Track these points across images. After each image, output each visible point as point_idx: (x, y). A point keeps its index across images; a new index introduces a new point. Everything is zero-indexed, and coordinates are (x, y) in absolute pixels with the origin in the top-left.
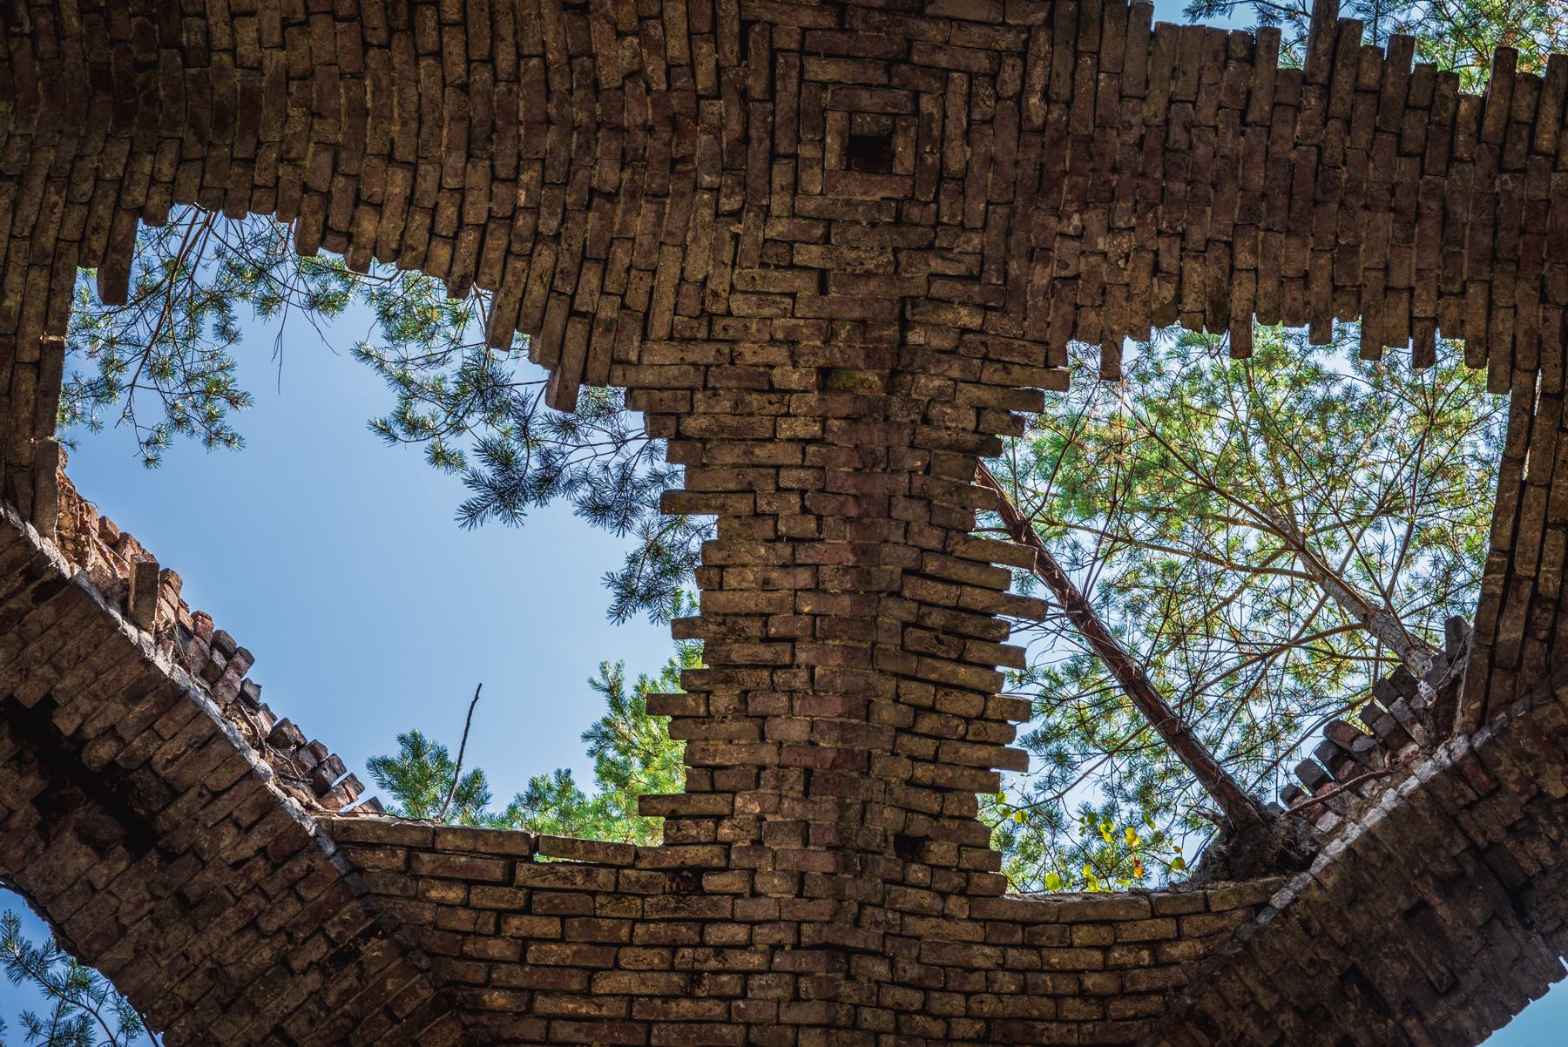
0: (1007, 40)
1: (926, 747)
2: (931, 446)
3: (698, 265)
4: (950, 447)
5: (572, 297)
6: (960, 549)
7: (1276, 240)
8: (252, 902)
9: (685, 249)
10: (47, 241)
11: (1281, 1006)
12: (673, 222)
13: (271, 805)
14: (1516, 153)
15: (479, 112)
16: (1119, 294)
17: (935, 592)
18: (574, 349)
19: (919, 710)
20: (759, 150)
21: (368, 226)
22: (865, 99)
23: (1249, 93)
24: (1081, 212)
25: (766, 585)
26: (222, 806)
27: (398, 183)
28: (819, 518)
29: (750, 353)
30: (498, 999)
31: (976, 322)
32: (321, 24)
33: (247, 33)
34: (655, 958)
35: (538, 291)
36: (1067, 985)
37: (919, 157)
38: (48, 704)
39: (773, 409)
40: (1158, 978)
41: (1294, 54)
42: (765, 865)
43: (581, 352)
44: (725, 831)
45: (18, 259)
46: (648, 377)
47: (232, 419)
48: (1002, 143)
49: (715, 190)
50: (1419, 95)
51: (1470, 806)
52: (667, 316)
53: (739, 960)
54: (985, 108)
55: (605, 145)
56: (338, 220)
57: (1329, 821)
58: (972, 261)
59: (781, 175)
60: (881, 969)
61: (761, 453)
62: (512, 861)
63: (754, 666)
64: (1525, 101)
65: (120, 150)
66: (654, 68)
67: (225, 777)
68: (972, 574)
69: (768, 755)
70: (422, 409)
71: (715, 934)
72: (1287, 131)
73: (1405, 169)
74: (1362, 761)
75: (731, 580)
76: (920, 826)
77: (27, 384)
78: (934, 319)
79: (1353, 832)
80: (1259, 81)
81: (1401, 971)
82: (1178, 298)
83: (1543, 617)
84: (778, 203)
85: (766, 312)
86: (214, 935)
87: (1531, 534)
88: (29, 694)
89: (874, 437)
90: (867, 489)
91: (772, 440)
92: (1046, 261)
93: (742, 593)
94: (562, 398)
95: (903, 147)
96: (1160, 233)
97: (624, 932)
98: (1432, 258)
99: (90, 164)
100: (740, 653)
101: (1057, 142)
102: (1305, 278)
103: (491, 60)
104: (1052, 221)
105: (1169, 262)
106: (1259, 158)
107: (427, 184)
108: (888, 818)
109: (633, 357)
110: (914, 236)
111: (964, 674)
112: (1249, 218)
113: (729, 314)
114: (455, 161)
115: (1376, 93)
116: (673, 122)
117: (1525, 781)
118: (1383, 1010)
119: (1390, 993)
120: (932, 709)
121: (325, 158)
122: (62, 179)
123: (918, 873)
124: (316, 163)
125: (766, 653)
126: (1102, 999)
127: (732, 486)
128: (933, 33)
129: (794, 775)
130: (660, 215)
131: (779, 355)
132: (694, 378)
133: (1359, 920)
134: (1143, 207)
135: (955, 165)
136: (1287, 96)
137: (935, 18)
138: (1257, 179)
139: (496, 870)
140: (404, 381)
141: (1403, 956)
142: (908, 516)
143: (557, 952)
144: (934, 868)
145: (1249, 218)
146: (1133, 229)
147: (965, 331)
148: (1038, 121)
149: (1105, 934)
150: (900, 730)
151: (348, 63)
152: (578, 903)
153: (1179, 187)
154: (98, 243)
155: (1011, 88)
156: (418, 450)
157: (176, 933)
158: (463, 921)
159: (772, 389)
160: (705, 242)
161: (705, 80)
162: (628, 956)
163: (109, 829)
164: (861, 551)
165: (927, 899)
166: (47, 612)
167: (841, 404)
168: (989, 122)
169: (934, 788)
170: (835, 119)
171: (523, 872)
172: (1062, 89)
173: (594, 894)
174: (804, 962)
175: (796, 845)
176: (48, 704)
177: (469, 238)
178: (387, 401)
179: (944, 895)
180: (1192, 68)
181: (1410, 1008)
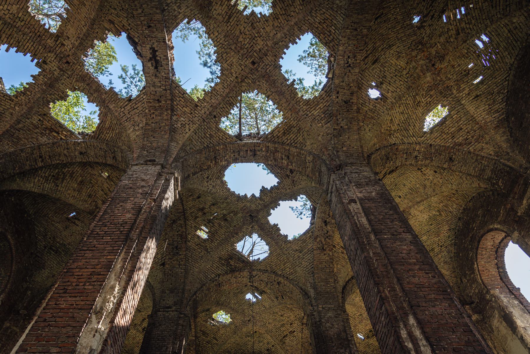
0: (270, 64)
1: (222, 111)
3: (234, 61)
7: (276, 95)
8: (161, 80)
10: (186, 14)
12: (235, 56)
13: (168, 74)
14: (298, 103)
15: (227, 34)
17: (232, 100)
19: (224, 107)
20: (246, 56)
21: (212, 35)
22: (256, 59)
26: (165, 71)
27: (217, 34)
29: (232, 71)
30: (175, 103)
32: (221, 16)
33: (215, 12)
34: (190, 109)
35: (221, 52)
36: (218, 136)
38: (157, 51)
40: (225, 141)
41: (289, 83)
42: (203, 109)
44: (202, 104)
45: (183, 13)
46: (223, 66)
47: (186, 40)
48: (263, 71)
50: (295, 93)
53: (196, 115)
54: (264, 67)
55: (235, 45)
56: (210, 33)
57: (246, 139)
59: (246, 59)
60: (206, 124)
61: (227, 79)
62: (184, 93)
65: (198, 12)
66: (243, 43)
67: (167, 69)
68: (235, 101)
69: (210, 101)
70: (201, 53)
71: (195, 111)
73: (290, 98)
74: (251, 137)
75: (217, 86)
76: (217, 116)
77: (175, 24)
79: (247, 141)
80: (285, 83)
81: (243, 154)
84: (244, 61)
86: (156, 80)
88: (156, 49)
89: (237, 85)
93: (217, 88)
94: (216, 61)
95: (256, 65)
98: (286, 106)
99: (195, 11)
100: (214, 92)
102: (276, 100)
103: (231, 31)
105: (268, 90)
107: (219, 36)
108: (215, 113)
111: (229, 107)
114: (223, 36)
116: (241, 48)
118: (239, 155)
119: (240, 155)
121: (213, 27)
122: (191, 10)
123: (214, 119)
124: (212, 27)
125: (216, 94)
128: (265, 58)
131: (235, 73)
132: (227, 69)
134: (269, 84)
135: (259, 70)
139: (182, 93)
140: (202, 49)
143: (182, 103)
151: (221, 21)
152: (187, 101)
153: (273, 85)
154: (190, 18)
155: (267, 67)
156: (198, 56)
157: (153, 77)
158: (177, 95)
161: (246, 47)
162: (187, 108)
163: (154, 65)
164: (229, 92)
165: (213, 122)
166: (163, 43)
167: (236, 80)
170: (253, 58)
171: (184, 95)
172: (271, 71)
174: (201, 119)
176: (157, 51)
177: (219, 43)
178: (199, 50)
181: (241, 157)
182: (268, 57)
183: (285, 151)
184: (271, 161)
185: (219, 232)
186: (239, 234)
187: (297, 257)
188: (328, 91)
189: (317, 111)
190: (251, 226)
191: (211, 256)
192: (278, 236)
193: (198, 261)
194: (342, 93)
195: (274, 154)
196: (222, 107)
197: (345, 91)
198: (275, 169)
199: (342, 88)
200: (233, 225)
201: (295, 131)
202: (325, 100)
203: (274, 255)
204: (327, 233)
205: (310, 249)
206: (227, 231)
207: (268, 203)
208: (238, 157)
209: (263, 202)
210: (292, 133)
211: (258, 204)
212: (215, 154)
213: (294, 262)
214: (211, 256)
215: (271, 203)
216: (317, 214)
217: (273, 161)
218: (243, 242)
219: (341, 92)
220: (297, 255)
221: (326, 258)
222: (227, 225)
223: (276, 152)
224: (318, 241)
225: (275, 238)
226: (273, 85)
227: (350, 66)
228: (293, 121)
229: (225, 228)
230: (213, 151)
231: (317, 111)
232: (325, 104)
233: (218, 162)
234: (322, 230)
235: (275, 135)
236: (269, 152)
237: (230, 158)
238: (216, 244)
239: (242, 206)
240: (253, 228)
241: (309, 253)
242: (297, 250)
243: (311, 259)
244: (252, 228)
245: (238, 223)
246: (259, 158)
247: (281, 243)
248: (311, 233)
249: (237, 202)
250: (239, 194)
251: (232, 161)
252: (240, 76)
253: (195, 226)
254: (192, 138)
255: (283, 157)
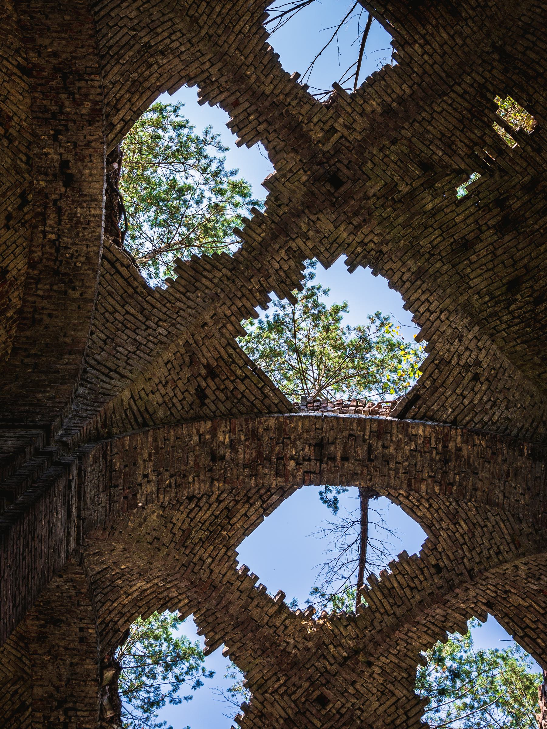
0: (277, 697)
2: (362, 631)
3: (376, 705)
4: (358, 627)
5: (404, 722)
6: (374, 607)
7: (257, 619)
9: (375, 710)
11: (390, 469)
12: (372, 719)
16: (298, 628)
18: (414, 711)
19: (411, 589)
20: (343, 720)
22: (314, 712)
23: (238, 649)
24: (291, 653)
25: (419, 637)
28: (396, 641)
29: (381, 680)
31: (331, 646)
37: (313, 691)
39: (386, 667)
41: (223, 648)
43: (414, 709)
46: (405, 692)
48: (295, 679)
49: (359, 718)
50: (204, 624)
51: (314, 473)
52: (391, 700)
54: (292, 689)
58: (321, 660)
59: (343, 711)
63: (436, 626)
64: (184, 610)
72: (237, 637)
76: (432, 570)
78: (338, 656)
80: (235, 649)
81: (359, 449)
82: (286, 618)
83: (265, 497)
84: (349, 705)
85: (370, 686)
87: (254, 517)
89: (370, 647)
90: (381, 640)
91: (391, 661)
92: (307, 646)
93: (426, 639)
96: (279, 636)
97: (512, 608)
98: (228, 595)
101: (284, 670)
102: (257, 606)
104: (298, 655)
105: (282, 628)
106: (246, 637)
109: (404, 698)
110: (328, 677)
112: (259, 627)
113: (378, 690)
115: (212, 630)
117: (298, 470)
118: (370, 446)
119: (365, 448)
120: (408, 586)
125: (432, 627)
126: (428, 500)
127: (408, 659)
128: (290, 712)
129: (448, 605)
130: (374, 722)
131: (375, 676)
133: (358, 469)
135: (308, 684)
136: (231, 642)
137: (287, 714)
138: (250, 635)
141: (355, 452)
142: (378, 624)
144: (437, 560)
145: (259, 627)
146: (284, 641)
147: (335, 647)
148: (284, 678)
149: (415, 509)
150: (419, 591)
152: (516, 619)
158: (542, 636)
159: (383, 670)
160: (370, 709)
164: (394, 631)
167: (372, 659)
168: (294, 685)
169: (423, 573)
170: (323, 712)
172: (274, 678)
173: (511, 618)
175: (460, 595)
179: (440, 553)
180: (245, 661)
181: (364, 441)
182: (283, 715)
183: (225, 472)
184: (267, 429)
185: (454, 122)
186: (379, 110)
187: (159, 30)
188: (111, 634)
189: (135, 588)
190: (337, 136)
191: (488, 35)
192: (236, 104)
193: (541, 20)
194: (71, 638)
195: (260, 454)
196: (415, 593)
197: (63, 643)
198: (256, 391)
199: (73, 649)
200: (401, 147)
201: (197, 531)
202: (116, 612)
203: (247, 17)
204: (58, 132)
205: (113, 62)
206: (425, 124)
207: (276, 247)
208: (373, 442)
209: (293, 245)
210: (207, 524)
211: (311, 234)
212: (445, 473)
213: (171, 15)
214: (488, 35)
215: (264, 245)
216: (100, 216)
217: (261, 430)
218: (366, 73)
219: (73, 641)
220: (160, 38)
221: (47, 42)
222: (424, 148)
223: (254, 460)
224: (88, 105)
225: (247, 96)
226: (267, 645)
227: (61, 703)
228: (206, 555)
229: (430, 136)
230: (452, 484)
231: (135, 588)
232: (115, 604)
233: (437, 439)
234: (75, 145)
235: (259, 503)
236: (274, 459)
237: (399, 441)
238: (468, 80)
239: (365, 230)
240: (327, 127)
241: (115, 49)
242: (162, 52)
243: (104, 31)
244: (333, 130)
245: (381, 156)
246: (305, 435)
247: (223, 79)
248: (115, 120)
249: (385, 249)
250: (375, 273)
251: (395, 431)
252: (360, 667)
253: (539, 150)
254: (513, 547)
255: (228, 451)
